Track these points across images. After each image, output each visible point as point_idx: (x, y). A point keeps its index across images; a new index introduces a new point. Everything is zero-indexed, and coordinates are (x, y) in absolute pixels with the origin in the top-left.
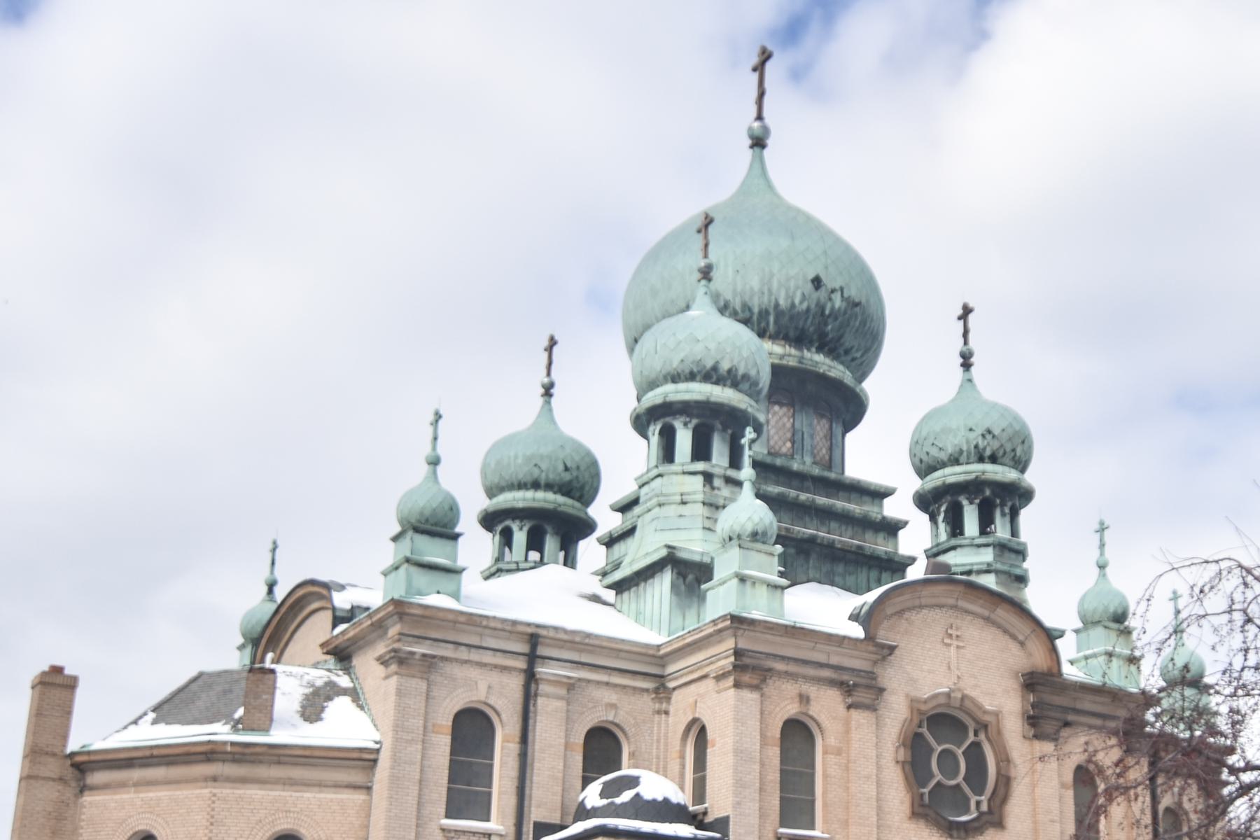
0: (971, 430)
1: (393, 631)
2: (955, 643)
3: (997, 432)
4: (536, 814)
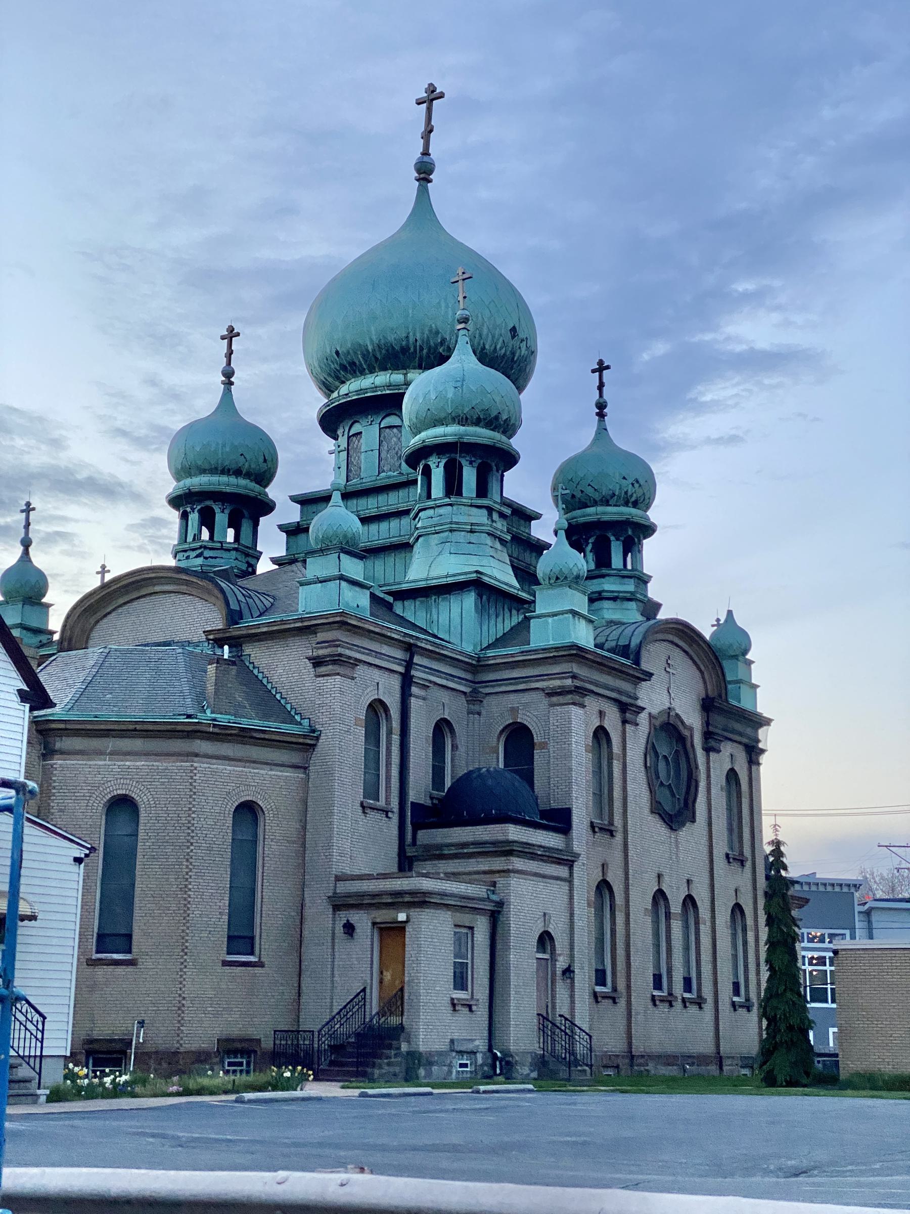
0: (624, 478)
3: (642, 482)
4: (413, 796)
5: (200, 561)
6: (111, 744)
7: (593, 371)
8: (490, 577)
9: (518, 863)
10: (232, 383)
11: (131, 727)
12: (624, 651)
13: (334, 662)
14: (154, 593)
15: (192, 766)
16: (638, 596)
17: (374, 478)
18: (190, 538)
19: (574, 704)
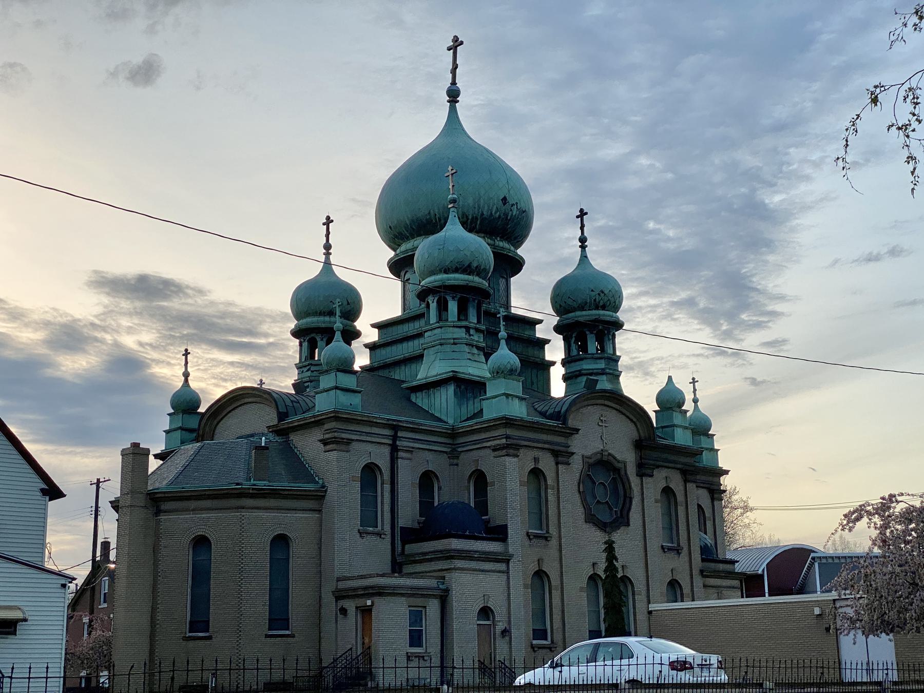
0: (592, 291)
2: (603, 424)
4: (402, 522)
5: (309, 374)
6: (193, 504)
7: (577, 217)
8: (463, 373)
9: (459, 563)
10: (330, 254)
12: (557, 416)
13: (332, 443)
14: (245, 403)
15: (241, 515)
16: (607, 370)
17: (417, 308)
18: (303, 360)
19: (507, 455)
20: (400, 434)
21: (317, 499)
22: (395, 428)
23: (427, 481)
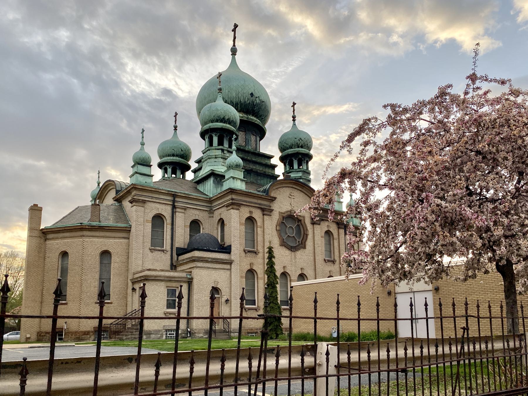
1: (133, 194)
10: (177, 130)
11: (64, 229)
19: (232, 209)
20: (177, 199)
21: (127, 232)
22: (174, 196)
23: (195, 225)
